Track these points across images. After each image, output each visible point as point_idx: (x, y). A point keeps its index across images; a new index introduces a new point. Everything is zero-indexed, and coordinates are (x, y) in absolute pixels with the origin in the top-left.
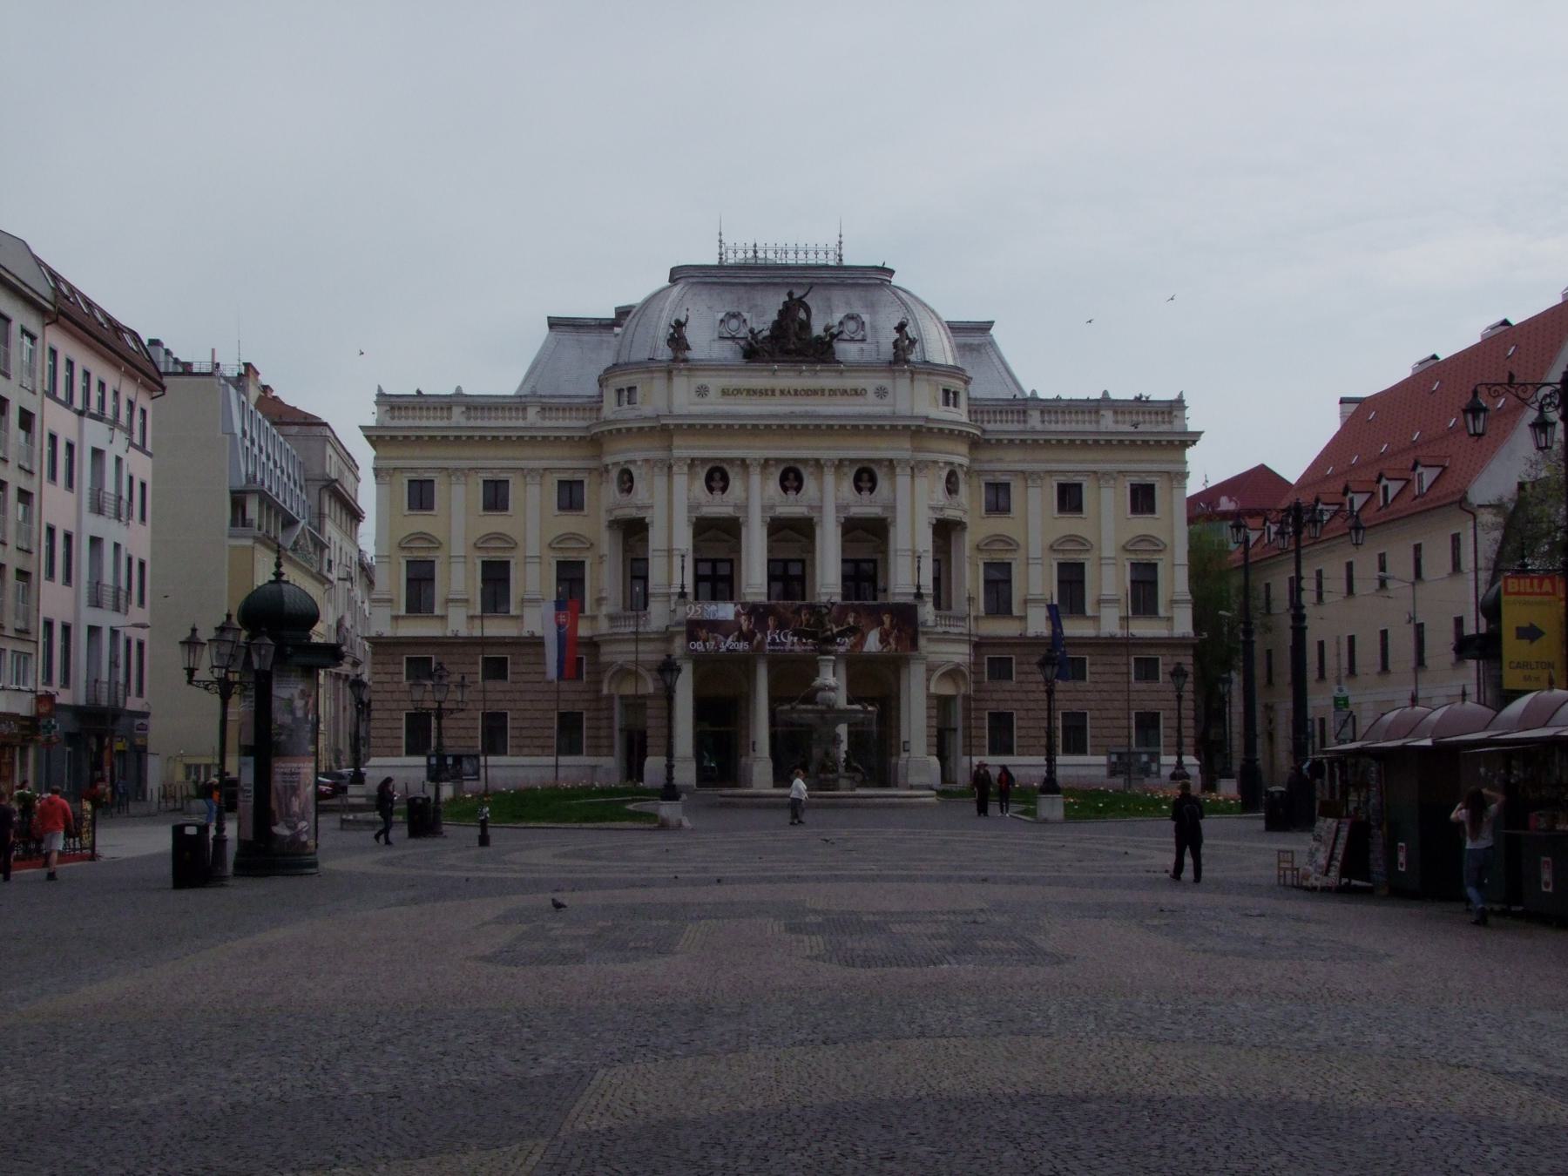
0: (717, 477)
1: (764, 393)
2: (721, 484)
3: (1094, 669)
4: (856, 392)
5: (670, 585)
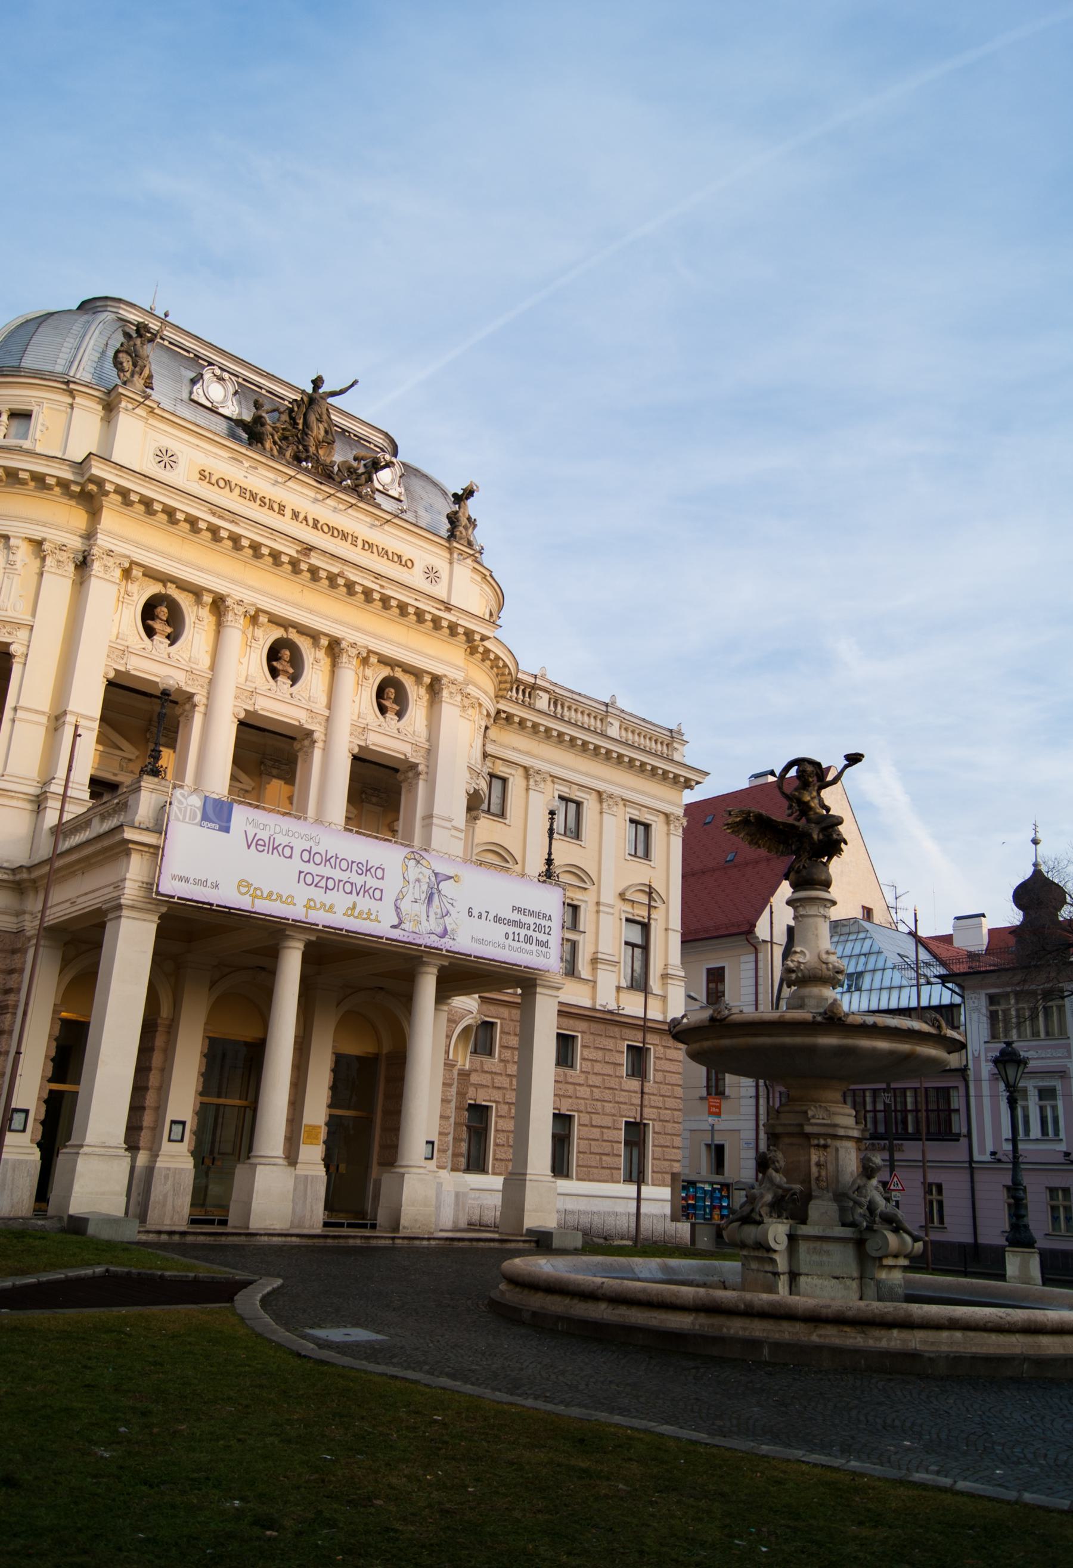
0: (160, 615)
1: (265, 503)
2: (169, 630)
5: (47, 783)
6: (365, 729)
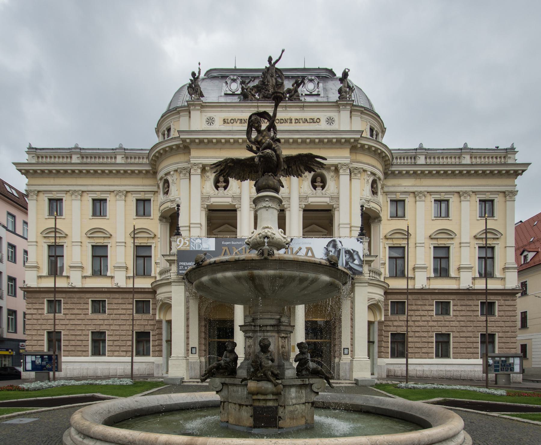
2: (224, 184)
3: (455, 308)
4: (313, 121)
6: (307, 198)
